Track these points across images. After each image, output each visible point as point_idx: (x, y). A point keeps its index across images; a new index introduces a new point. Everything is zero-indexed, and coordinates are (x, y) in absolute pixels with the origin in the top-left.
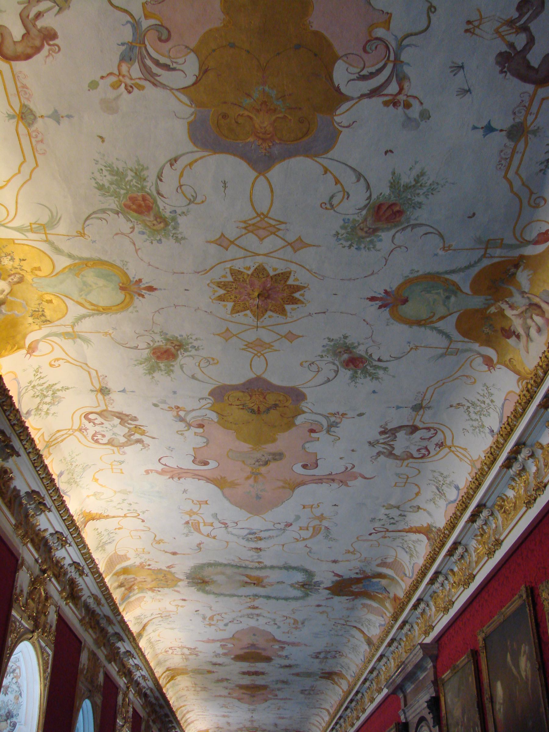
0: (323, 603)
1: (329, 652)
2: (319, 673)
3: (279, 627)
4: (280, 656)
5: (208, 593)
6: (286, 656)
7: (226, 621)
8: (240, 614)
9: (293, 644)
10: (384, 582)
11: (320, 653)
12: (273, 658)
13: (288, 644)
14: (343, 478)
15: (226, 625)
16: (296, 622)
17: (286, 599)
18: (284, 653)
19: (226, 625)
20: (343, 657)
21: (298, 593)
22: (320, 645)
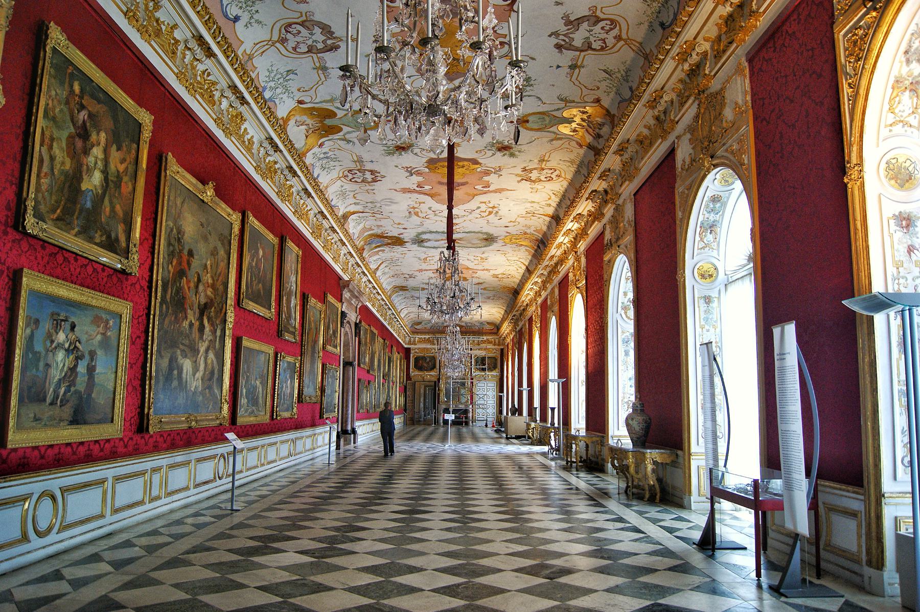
0: (403, 231)
1: (363, 181)
2: (346, 129)
3: (430, 208)
4: (419, 173)
5: (486, 233)
6: (412, 175)
7: (478, 211)
8: (465, 218)
9: (410, 191)
10: (374, 245)
11: (374, 181)
12: (427, 170)
13: (414, 191)
14: (421, 271)
15: (479, 208)
16: (417, 214)
17: (431, 232)
18: (416, 179)
19: (479, 208)
20: (341, 175)
21: (424, 237)
22: (382, 190)
